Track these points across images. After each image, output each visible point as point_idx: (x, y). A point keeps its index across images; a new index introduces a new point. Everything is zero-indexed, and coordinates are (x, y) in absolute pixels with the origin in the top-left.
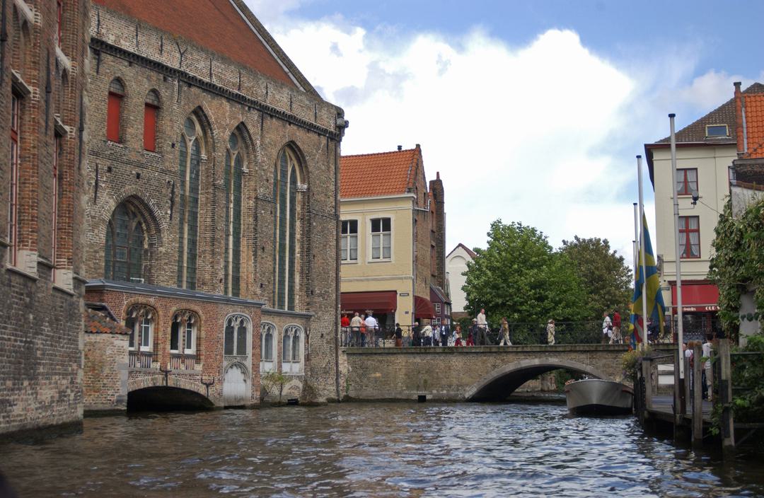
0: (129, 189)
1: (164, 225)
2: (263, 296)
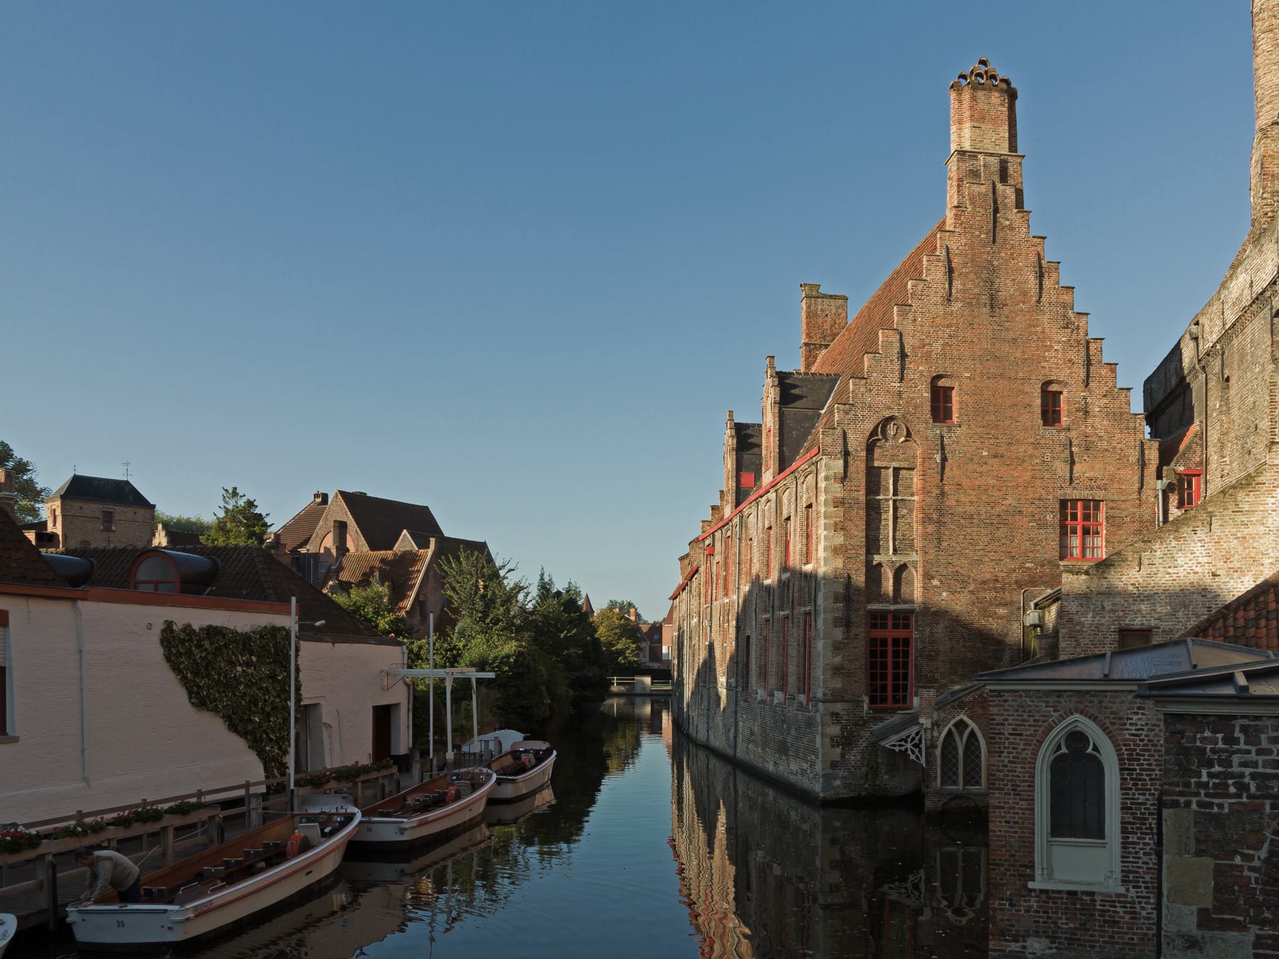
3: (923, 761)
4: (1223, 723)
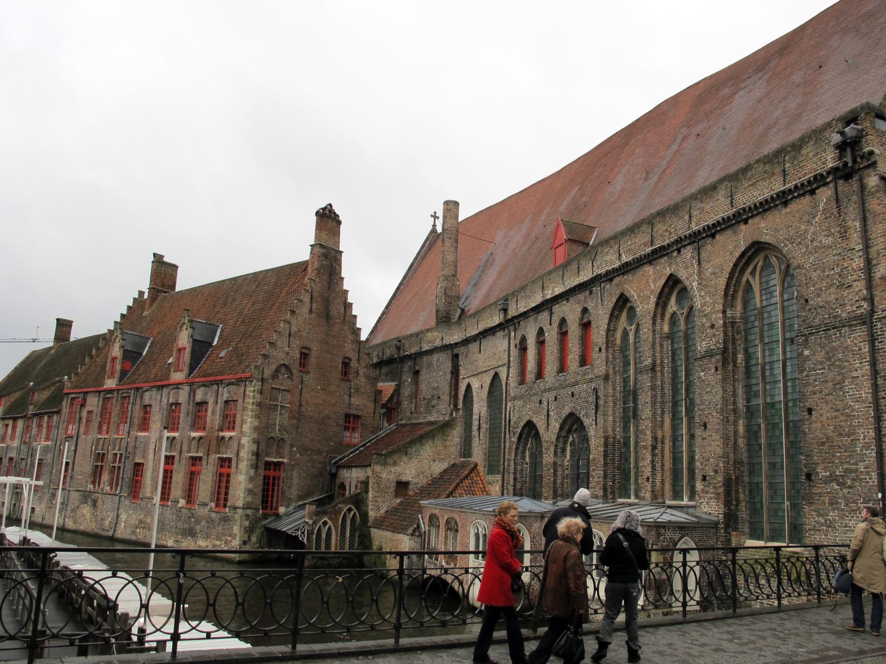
0: (566, 411)
1: (591, 432)
2: (707, 492)
3: (305, 541)
4: (664, 527)
